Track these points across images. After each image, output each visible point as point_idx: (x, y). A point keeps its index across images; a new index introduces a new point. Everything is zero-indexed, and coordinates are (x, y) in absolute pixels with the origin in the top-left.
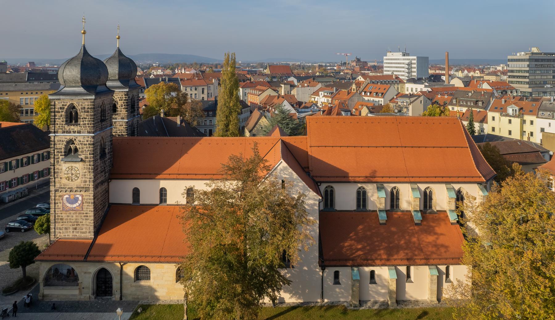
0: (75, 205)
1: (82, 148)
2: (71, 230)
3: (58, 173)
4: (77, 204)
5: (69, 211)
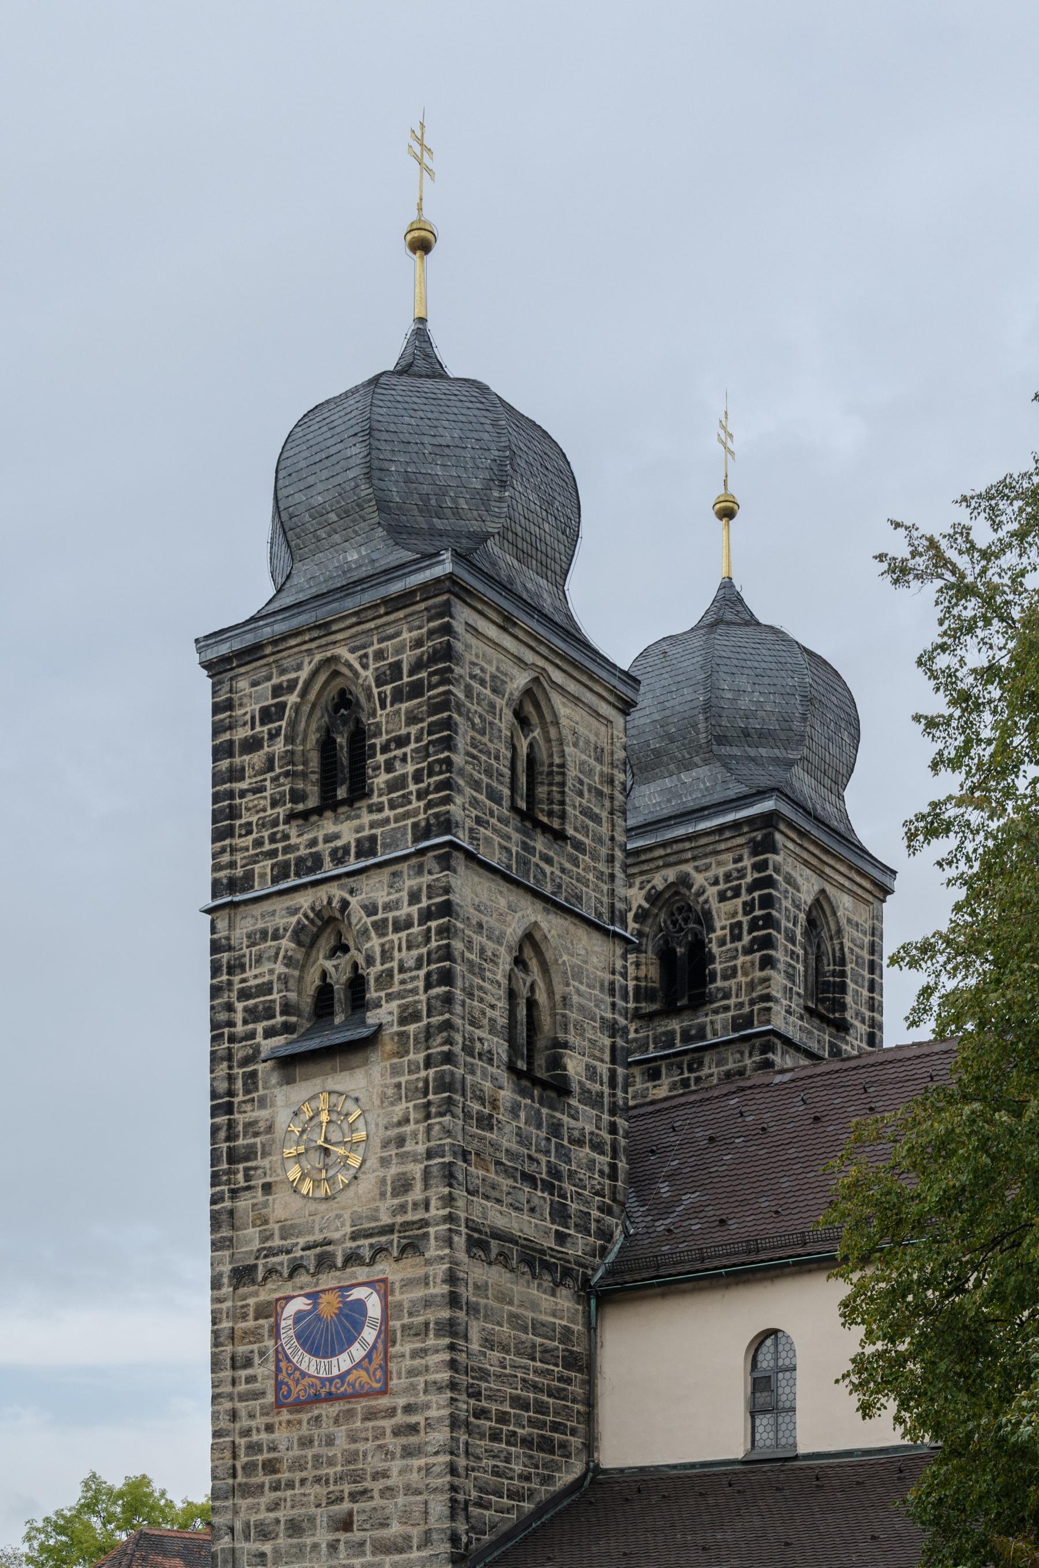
0: (343, 1362)
1: (386, 955)
2: (323, 1536)
3: (250, 1154)
4: (358, 1351)
5: (316, 1399)
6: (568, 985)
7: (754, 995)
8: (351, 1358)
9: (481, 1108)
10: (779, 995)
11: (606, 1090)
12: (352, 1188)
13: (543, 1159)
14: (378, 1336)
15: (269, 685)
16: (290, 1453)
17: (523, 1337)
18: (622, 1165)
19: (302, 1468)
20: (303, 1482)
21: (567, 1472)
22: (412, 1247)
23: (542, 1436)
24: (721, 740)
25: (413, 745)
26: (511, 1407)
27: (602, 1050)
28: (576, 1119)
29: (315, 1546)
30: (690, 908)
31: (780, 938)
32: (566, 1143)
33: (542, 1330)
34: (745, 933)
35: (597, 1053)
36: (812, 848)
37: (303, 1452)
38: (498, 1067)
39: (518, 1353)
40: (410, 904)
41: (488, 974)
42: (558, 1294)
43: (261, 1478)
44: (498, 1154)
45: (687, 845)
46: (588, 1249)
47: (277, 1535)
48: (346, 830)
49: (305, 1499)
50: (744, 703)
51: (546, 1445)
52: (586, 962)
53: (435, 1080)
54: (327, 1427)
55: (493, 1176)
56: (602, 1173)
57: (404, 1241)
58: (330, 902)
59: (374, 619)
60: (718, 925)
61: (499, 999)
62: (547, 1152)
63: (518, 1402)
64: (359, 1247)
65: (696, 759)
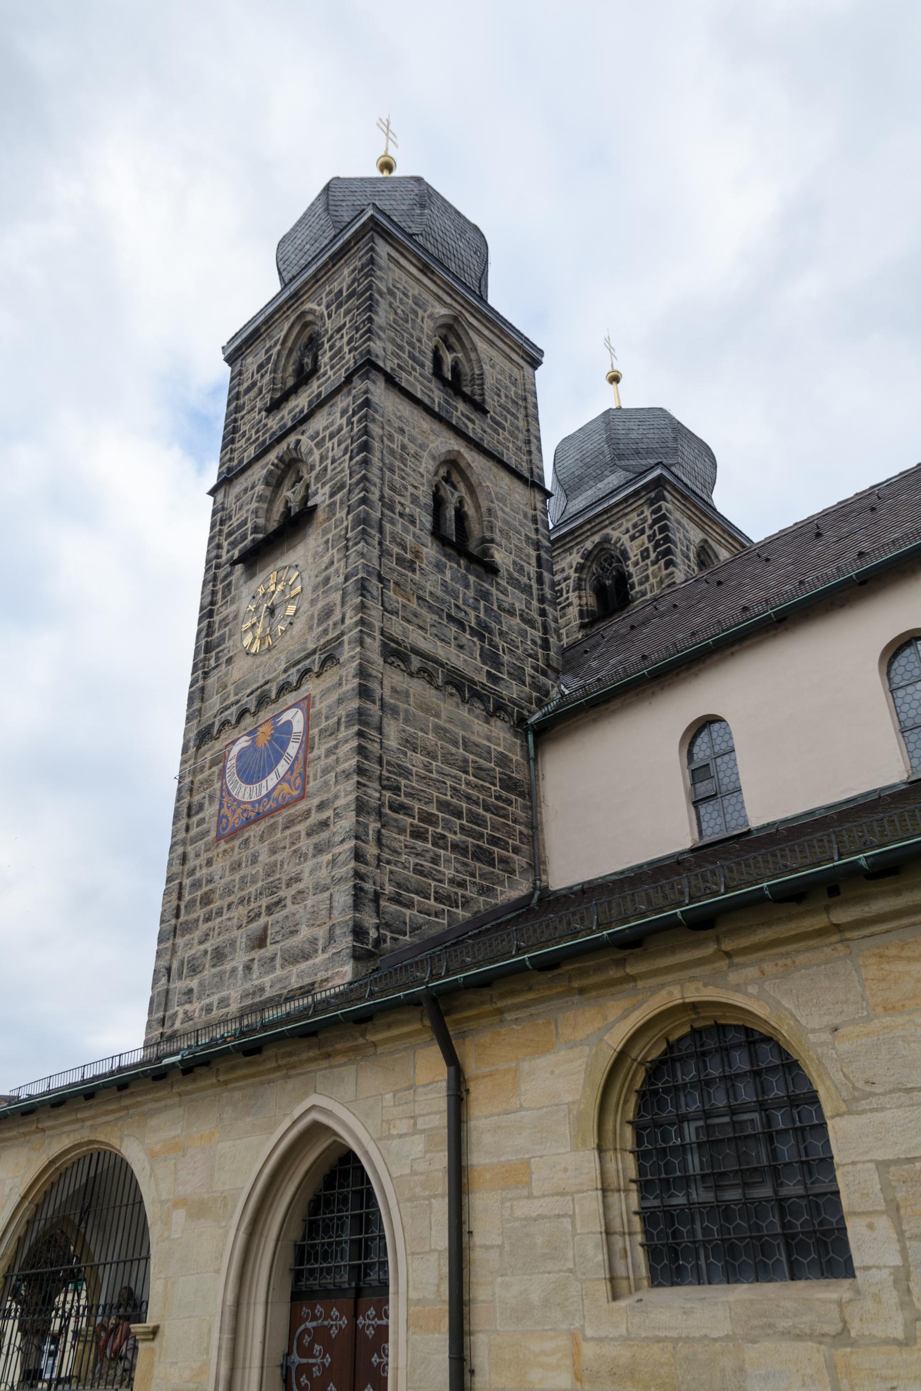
0: (272, 780)
4: (282, 767)
5: (249, 823)
6: (493, 502)
7: (663, 586)
9: (402, 552)
13: (472, 614)
14: (300, 748)
17: (453, 750)
21: (511, 887)
22: (330, 659)
23: (479, 847)
24: (620, 456)
26: (438, 810)
27: (528, 556)
28: (507, 596)
30: (612, 557)
31: (678, 551)
32: (495, 608)
33: (474, 749)
35: (524, 557)
36: (693, 509)
38: (421, 530)
39: (446, 762)
41: (409, 463)
42: (492, 723)
44: (421, 592)
45: (605, 517)
46: (523, 695)
48: (301, 402)
50: (633, 435)
53: (353, 521)
54: (255, 846)
56: (534, 642)
58: (288, 448)
59: (326, 273)
60: (631, 555)
61: (423, 484)
62: (476, 609)
63: (443, 805)
65: (606, 473)
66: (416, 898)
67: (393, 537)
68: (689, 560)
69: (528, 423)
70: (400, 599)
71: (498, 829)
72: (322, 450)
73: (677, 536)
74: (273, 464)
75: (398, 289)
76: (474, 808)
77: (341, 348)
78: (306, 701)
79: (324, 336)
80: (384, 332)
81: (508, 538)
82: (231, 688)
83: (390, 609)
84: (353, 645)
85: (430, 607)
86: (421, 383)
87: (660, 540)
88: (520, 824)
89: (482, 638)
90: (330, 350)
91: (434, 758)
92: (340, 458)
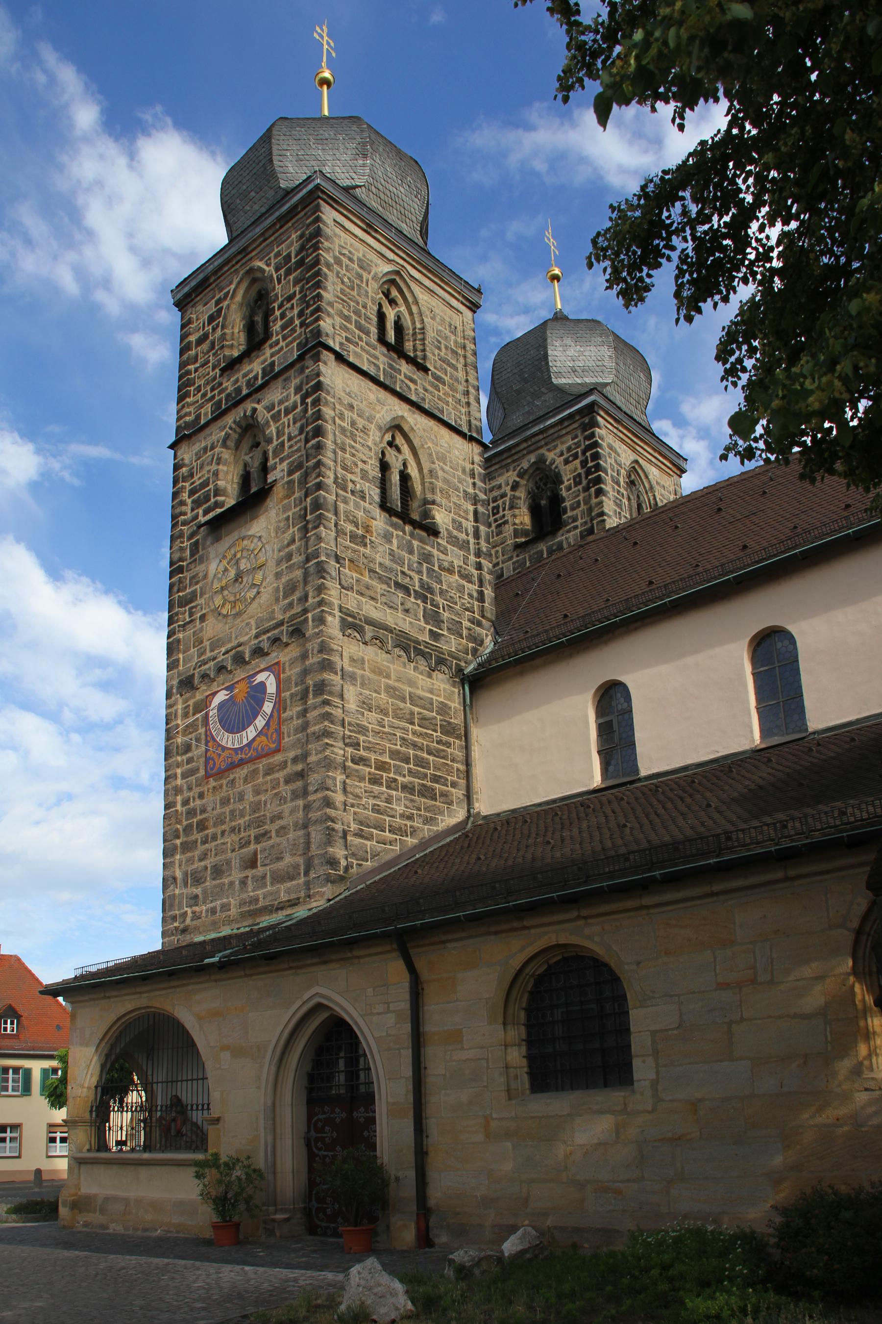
0: (251, 733)
4: (260, 722)
5: (233, 766)
6: (433, 463)
8: (256, 728)
9: (355, 529)
10: (611, 513)
11: (472, 540)
12: (257, 601)
13: (416, 578)
15: (213, 301)
16: (215, 812)
17: (402, 705)
18: (489, 592)
19: (223, 822)
20: (223, 833)
21: (449, 816)
23: (423, 785)
25: (298, 297)
26: (390, 758)
27: (466, 512)
29: (231, 884)
30: (547, 477)
31: (608, 479)
32: (436, 568)
33: (420, 702)
34: (583, 479)
35: (462, 514)
36: (625, 432)
37: (223, 810)
38: (370, 504)
39: (396, 716)
40: (295, 394)
41: (358, 439)
42: (434, 676)
43: (197, 836)
45: (541, 437)
46: (460, 648)
47: (206, 879)
48: (255, 367)
49: (224, 847)
51: (427, 792)
52: (449, 452)
53: (311, 504)
54: (240, 787)
55: (367, 579)
56: (471, 596)
57: (291, 629)
58: (245, 414)
59: (274, 234)
60: (565, 479)
61: (371, 458)
62: (420, 572)
63: (394, 754)
64: (260, 642)
65: (543, 390)
66: (375, 831)
67: (347, 516)
68: (619, 486)
69: (467, 373)
70: (355, 575)
71: (439, 769)
72: (278, 425)
73: (607, 462)
74: (231, 428)
75: (344, 255)
76: (419, 753)
77: (292, 319)
78: (277, 667)
79: (274, 301)
80: (332, 307)
81: (448, 497)
82: (207, 644)
83: (346, 585)
84: (316, 623)
85: (380, 578)
86: (367, 352)
87: (591, 467)
88: (457, 762)
89: (425, 599)
90: (282, 319)
91: (386, 714)
92: (296, 437)
